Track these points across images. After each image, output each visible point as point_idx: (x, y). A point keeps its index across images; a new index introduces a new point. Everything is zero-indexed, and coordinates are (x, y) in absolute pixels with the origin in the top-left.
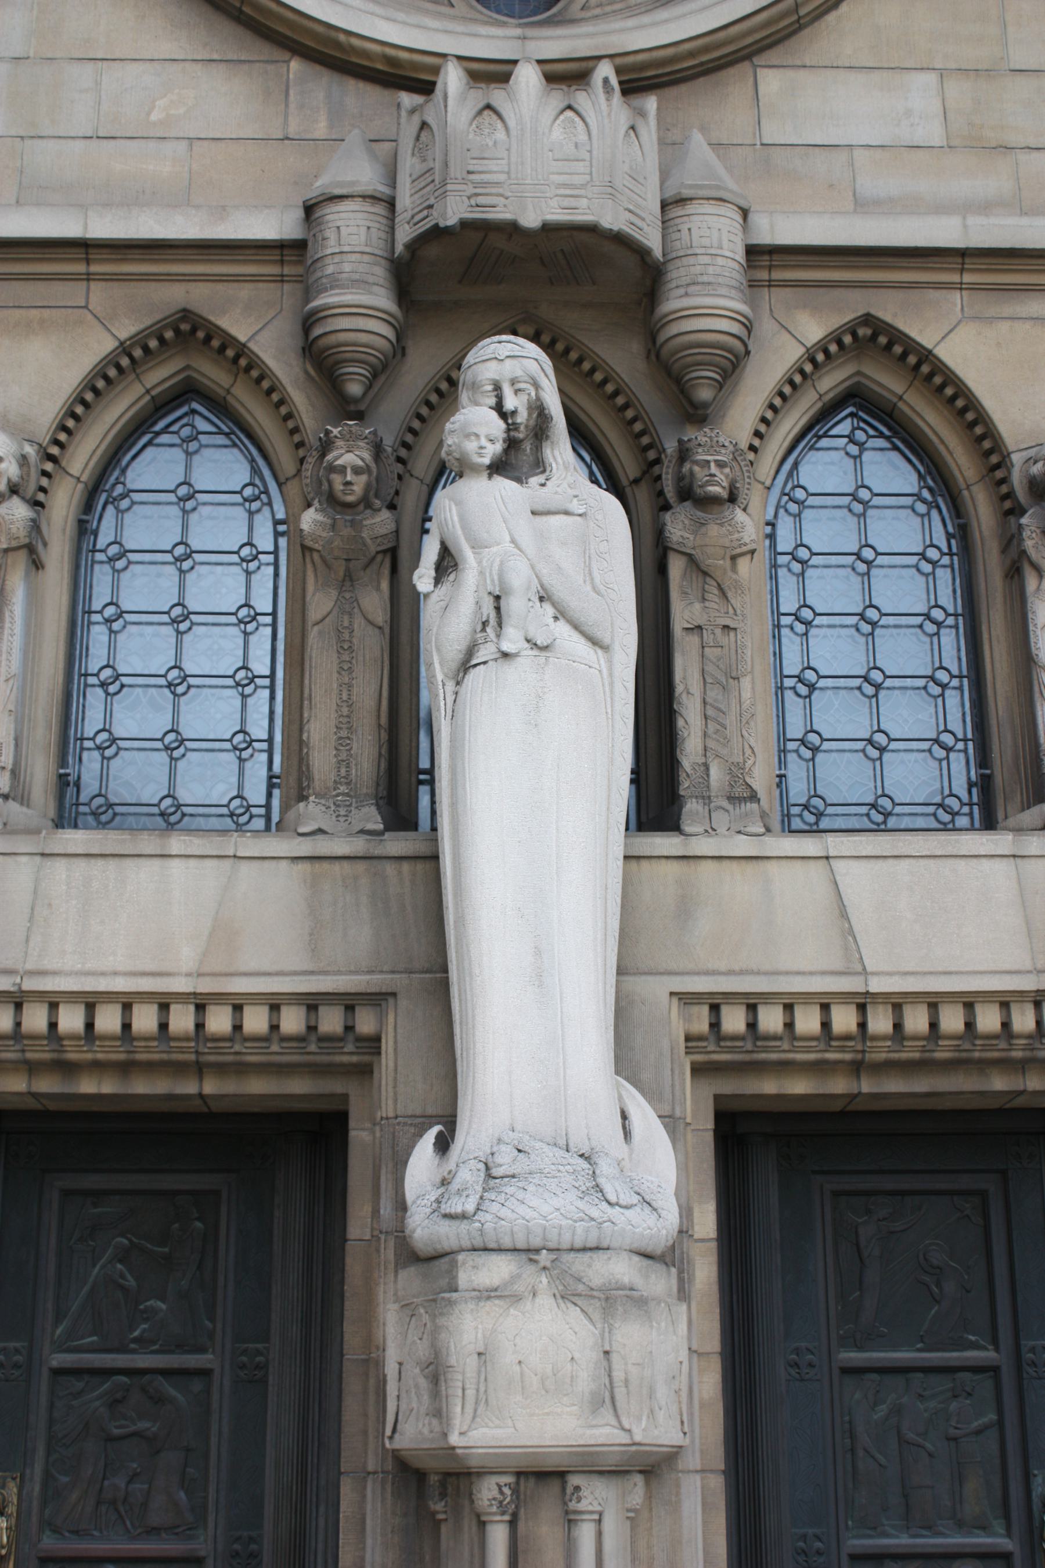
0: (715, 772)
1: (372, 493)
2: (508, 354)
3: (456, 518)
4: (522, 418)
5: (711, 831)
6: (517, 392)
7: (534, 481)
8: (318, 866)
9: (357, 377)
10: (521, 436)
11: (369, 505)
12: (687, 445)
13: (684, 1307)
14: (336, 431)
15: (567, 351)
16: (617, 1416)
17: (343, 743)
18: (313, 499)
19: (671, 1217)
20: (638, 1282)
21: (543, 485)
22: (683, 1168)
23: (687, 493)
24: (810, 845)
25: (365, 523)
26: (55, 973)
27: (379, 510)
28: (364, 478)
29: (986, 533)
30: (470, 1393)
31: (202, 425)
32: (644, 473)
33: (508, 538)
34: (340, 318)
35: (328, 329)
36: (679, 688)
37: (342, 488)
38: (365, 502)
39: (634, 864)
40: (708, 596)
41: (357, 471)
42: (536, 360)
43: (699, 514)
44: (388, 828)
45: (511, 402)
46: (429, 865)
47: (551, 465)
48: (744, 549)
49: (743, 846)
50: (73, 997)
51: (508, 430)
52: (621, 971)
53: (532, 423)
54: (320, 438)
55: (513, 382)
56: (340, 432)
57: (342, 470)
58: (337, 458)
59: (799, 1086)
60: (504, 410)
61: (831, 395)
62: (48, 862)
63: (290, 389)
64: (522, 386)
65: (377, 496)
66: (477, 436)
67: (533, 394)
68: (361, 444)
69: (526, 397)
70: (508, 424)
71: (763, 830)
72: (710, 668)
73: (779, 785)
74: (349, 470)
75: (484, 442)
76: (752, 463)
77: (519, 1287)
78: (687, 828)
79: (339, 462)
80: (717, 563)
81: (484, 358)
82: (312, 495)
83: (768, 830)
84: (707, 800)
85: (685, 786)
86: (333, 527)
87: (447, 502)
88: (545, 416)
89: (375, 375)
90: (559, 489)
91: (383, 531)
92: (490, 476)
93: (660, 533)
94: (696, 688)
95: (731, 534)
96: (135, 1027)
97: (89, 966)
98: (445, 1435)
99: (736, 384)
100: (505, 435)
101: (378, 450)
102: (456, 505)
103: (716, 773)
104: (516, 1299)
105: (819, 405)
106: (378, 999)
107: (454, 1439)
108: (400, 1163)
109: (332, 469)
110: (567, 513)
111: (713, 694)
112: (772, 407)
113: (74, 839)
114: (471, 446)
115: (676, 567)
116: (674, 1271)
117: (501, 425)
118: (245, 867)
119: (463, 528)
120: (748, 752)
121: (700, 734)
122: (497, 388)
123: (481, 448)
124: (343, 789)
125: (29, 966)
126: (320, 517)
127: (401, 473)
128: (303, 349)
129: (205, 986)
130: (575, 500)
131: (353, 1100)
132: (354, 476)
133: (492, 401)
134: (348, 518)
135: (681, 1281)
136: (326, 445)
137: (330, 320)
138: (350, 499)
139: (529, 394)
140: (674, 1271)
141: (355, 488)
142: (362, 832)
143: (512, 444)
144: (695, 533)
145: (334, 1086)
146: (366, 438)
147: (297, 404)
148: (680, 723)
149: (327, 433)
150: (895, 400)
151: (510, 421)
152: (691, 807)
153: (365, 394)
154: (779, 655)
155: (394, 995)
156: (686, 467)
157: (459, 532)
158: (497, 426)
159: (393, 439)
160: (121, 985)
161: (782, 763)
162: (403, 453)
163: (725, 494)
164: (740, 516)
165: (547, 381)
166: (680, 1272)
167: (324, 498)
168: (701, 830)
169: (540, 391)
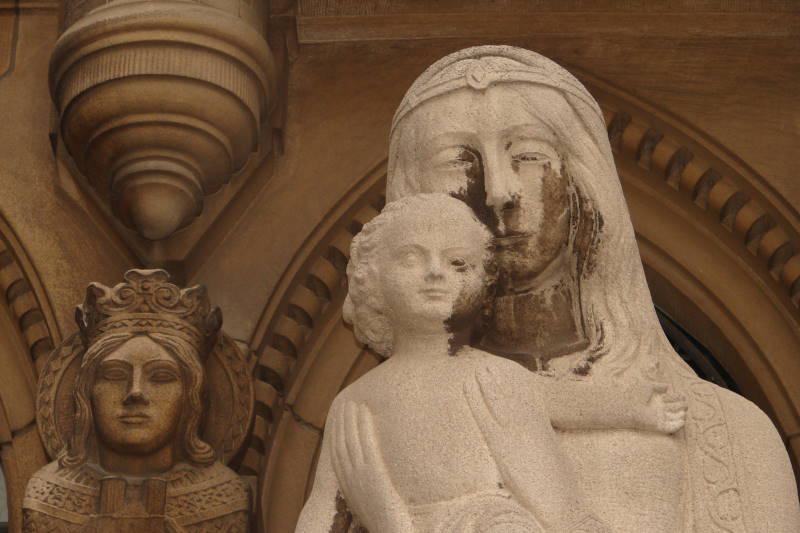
1: (192, 425)
2: (496, 77)
3: (372, 441)
4: (531, 219)
6: (517, 162)
7: (562, 365)
9: (164, 180)
10: (530, 263)
11: (185, 454)
14: (110, 293)
15: (651, 140)
18: (57, 450)
21: (583, 372)
25: (171, 490)
27: (208, 464)
28: (173, 391)
33: (494, 477)
34: (130, 53)
35: (100, 79)
37: (120, 411)
38: (176, 446)
41: (157, 375)
42: (562, 92)
45: (502, 184)
47: (601, 329)
51: (496, 248)
53: (554, 234)
54: (78, 312)
55: (508, 139)
56: (119, 293)
57: (124, 372)
58: (111, 348)
60: (489, 202)
63: (20, 227)
64: (530, 147)
65: (202, 434)
66: (424, 253)
67: (556, 166)
68: (169, 317)
69: (540, 173)
70: (497, 234)
74: (138, 373)
75: (437, 264)
79: (116, 356)
81: (441, 89)
82: (56, 442)
86: (99, 502)
87: (353, 407)
88: (586, 216)
89: (210, 186)
90: (620, 381)
91: (216, 510)
92: (455, 348)
100: (487, 256)
101: (210, 340)
102: (373, 411)
109: (101, 371)
110: (638, 427)
114: (409, 277)
117: (485, 234)
119: (388, 460)
122: (473, 156)
123: (433, 277)
126: (68, 481)
127: (269, 401)
128: (53, 138)
130: (658, 400)
132: (149, 386)
133: (461, 183)
134: (130, 479)
136: (91, 321)
137: (106, 59)
138: (139, 435)
139: (546, 167)
141: (151, 411)
143: (504, 281)
146: (181, 304)
147: (36, 257)
149: (92, 295)
151: (502, 227)
153: (186, 222)
157: (380, 468)
158: (468, 233)
159: (250, 325)
162: (273, 359)
165: (588, 140)
167: (80, 438)
169: (573, 161)
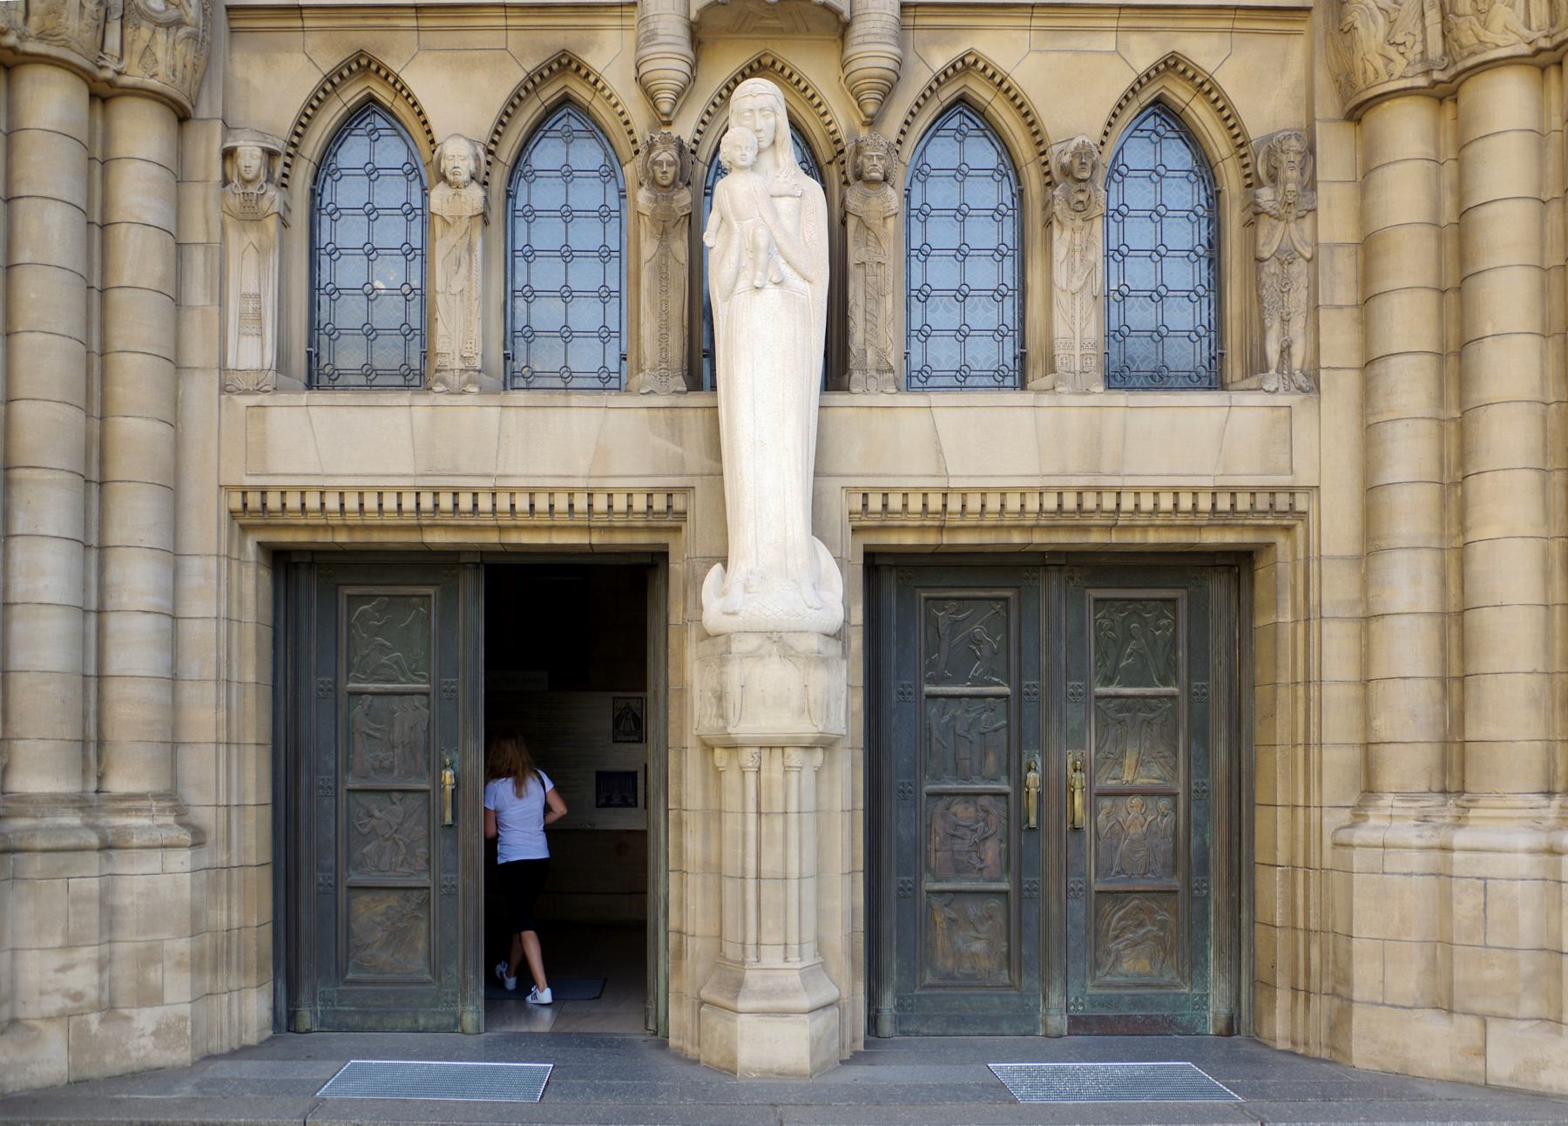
0: (869, 353)
5: (866, 391)
8: (652, 411)
12: (861, 145)
13: (845, 662)
16: (811, 718)
17: (663, 337)
19: (838, 614)
20: (822, 649)
22: (846, 587)
23: (859, 176)
24: (920, 400)
26: (513, 476)
29: (1034, 196)
30: (738, 706)
31: (576, 125)
32: (835, 157)
36: (851, 302)
39: (823, 410)
40: (869, 243)
43: (867, 190)
44: (688, 390)
46: (712, 411)
48: (892, 213)
49: (884, 400)
50: (523, 489)
52: (816, 474)
59: (909, 539)
61: (948, 102)
62: (506, 411)
71: (894, 391)
72: (869, 289)
73: (906, 358)
76: (897, 152)
77: (762, 652)
78: (853, 390)
80: (876, 222)
83: (899, 390)
84: (864, 371)
85: (853, 363)
93: (843, 203)
94: (861, 302)
95: (884, 203)
96: (556, 508)
97: (531, 472)
98: (725, 728)
99: (891, 98)
103: (871, 356)
104: (762, 657)
105: (941, 108)
106: (686, 490)
107: (729, 730)
108: (699, 582)
111: (871, 306)
112: (912, 113)
113: (519, 397)
115: (852, 223)
116: (840, 642)
118: (612, 414)
120: (889, 342)
121: (862, 330)
124: (664, 365)
125: (499, 472)
129: (593, 483)
131: (670, 546)
135: (844, 648)
140: (840, 642)
142: (675, 392)
144: (863, 203)
145: (660, 538)
148: (851, 324)
150: (986, 104)
152: (856, 375)
154: (909, 276)
155: (693, 488)
156: (860, 158)
160: (548, 483)
161: (908, 344)
163: (881, 178)
164: (890, 191)
166: (844, 643)
168: (861, 390)
